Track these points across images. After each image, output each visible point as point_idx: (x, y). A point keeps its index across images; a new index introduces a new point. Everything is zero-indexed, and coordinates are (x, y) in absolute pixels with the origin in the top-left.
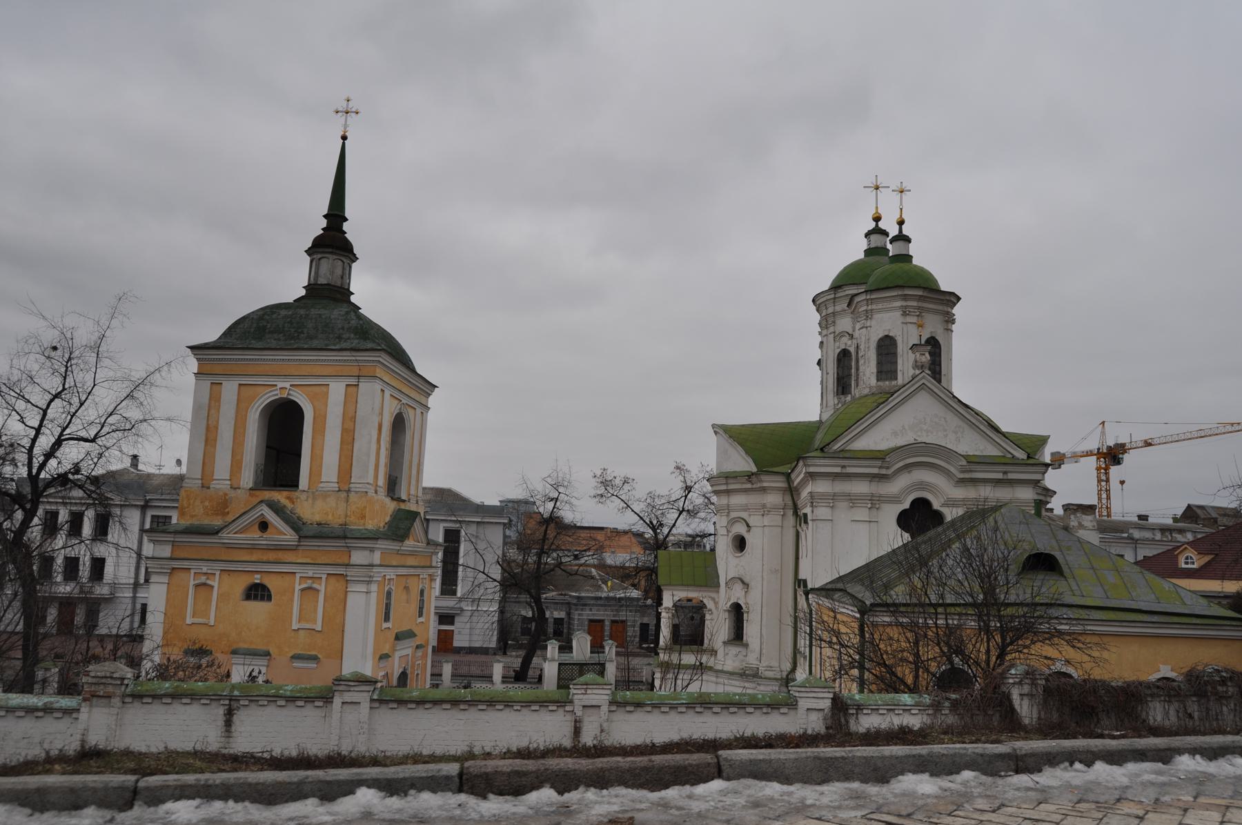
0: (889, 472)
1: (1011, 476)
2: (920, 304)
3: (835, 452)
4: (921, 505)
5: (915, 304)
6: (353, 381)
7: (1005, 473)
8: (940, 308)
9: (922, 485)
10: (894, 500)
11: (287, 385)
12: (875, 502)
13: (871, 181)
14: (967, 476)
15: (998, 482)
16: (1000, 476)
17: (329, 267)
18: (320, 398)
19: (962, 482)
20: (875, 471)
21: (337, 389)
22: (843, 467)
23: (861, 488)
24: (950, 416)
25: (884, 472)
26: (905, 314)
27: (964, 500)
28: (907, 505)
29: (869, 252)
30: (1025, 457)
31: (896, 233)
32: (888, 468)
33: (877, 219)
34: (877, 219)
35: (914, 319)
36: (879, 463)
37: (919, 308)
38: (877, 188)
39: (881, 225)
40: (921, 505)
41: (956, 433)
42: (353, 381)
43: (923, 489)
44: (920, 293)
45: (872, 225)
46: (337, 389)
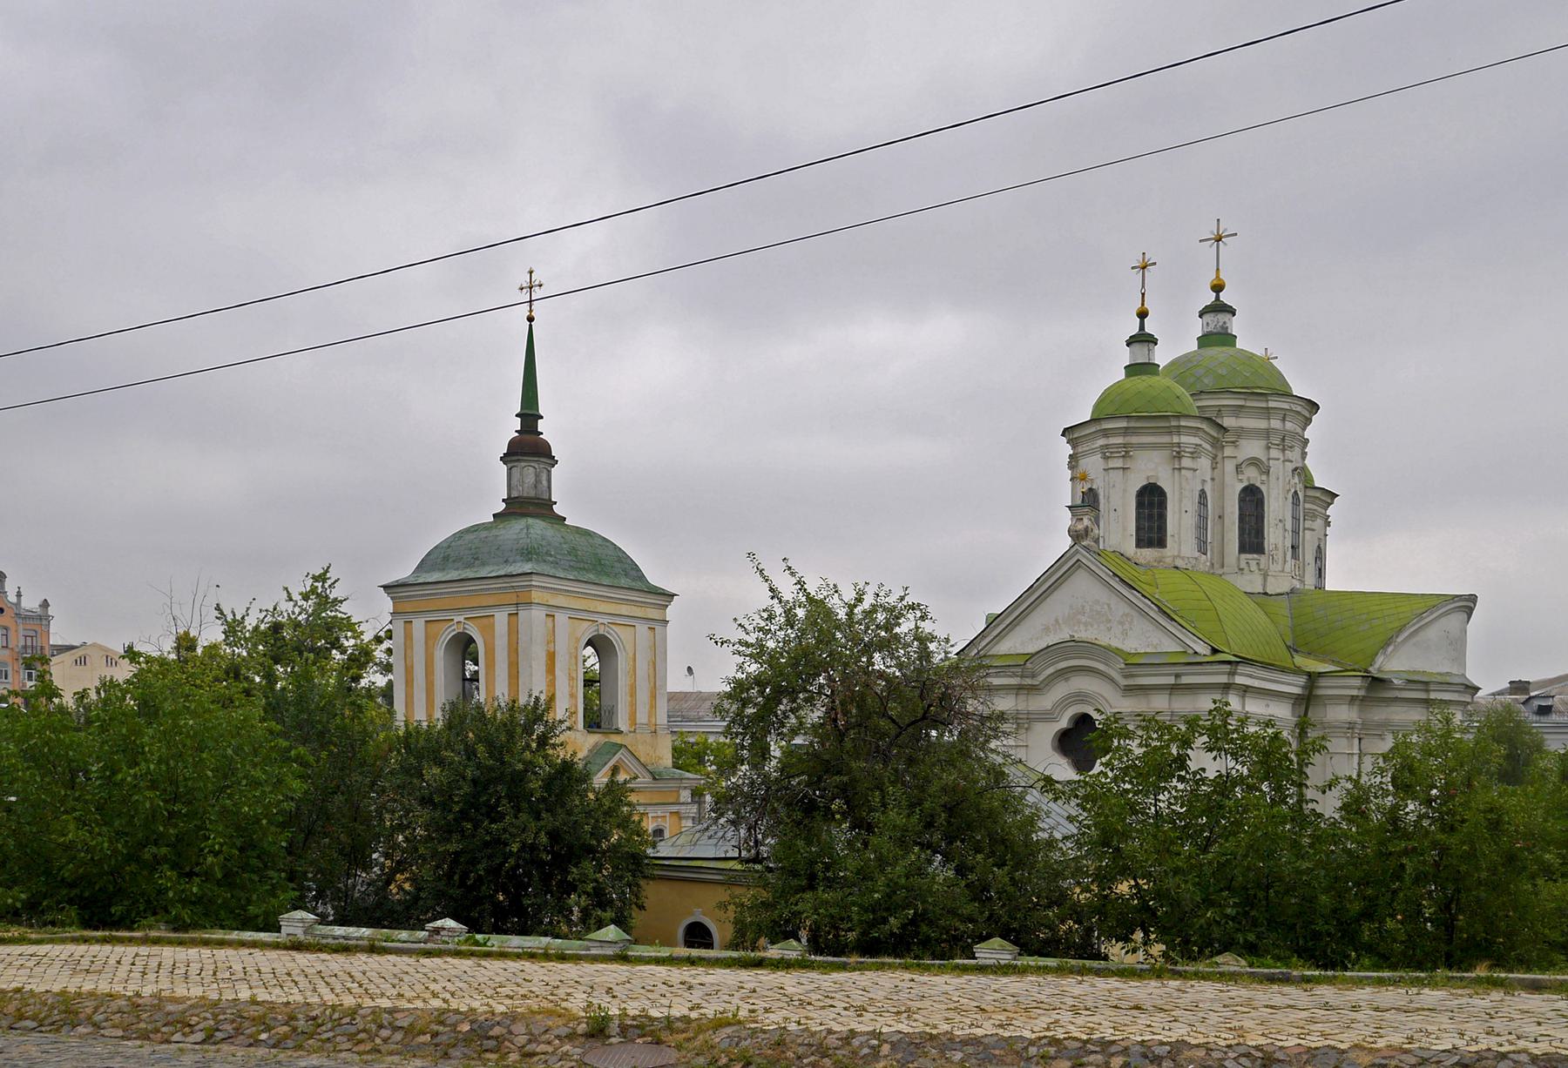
1: (1185, 680)
5: (1119, 440)
6: (513, 610)
7: (1177, 676)
8: (1165, 439)
9: (1080, 697)
10: (1046, 717)
11: (461, 619)
14: (1131, 682)
15: (1174, 689)
16: (1172, 680)
17: (528, 471)
18: (489, 631)
19: (1130, 690)
21: (501, 618)
24: (1114, 601)
25: (1028, 681)
26: (1106, 458)
28: (1064, 723)
29: (1205, 340)
30: (1208, 651)
32: (1033, 676)
35: (1119, 463)
37: (1125, 445)
40: (1083, 721)
41: (1121, 623)
42: (513, 610)
46: (501, 618)
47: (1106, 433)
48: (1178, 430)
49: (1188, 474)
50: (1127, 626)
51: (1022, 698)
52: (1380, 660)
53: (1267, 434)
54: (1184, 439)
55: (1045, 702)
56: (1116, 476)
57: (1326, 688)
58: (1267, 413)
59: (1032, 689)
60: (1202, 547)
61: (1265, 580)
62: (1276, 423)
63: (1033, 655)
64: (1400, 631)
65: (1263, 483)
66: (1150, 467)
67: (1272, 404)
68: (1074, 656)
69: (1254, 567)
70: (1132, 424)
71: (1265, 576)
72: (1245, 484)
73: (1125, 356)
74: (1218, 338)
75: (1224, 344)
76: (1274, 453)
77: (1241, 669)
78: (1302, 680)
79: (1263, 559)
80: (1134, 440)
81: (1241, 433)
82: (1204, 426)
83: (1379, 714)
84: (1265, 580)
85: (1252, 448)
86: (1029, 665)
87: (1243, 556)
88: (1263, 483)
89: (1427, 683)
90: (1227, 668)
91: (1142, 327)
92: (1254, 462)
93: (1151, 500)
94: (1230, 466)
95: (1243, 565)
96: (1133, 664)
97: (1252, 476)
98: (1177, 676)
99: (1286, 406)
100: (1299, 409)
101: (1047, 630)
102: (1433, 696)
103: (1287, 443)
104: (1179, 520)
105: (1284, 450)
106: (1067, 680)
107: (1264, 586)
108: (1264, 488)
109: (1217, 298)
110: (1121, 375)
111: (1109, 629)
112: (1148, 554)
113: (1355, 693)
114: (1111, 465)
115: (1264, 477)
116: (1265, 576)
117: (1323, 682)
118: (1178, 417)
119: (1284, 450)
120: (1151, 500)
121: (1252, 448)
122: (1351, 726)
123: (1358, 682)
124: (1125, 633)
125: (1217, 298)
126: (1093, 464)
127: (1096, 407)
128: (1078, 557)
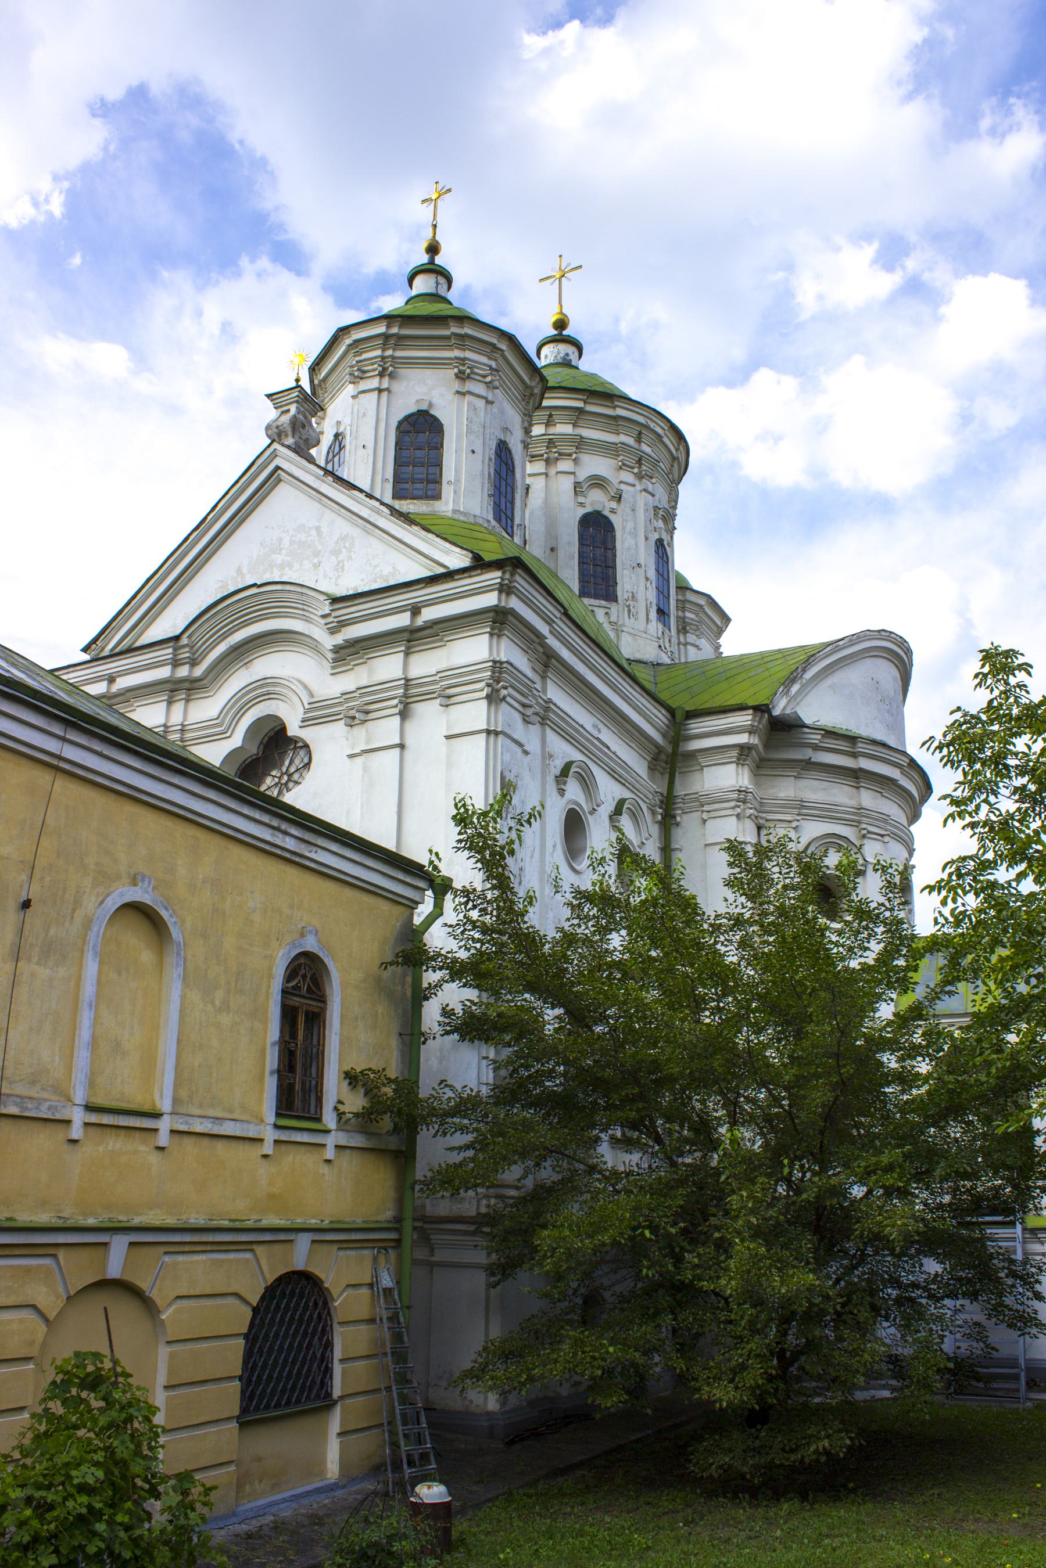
13: (551, 268)
16: (403, 620)
25: (183, 672)
32: (194, 663)
41: (336, 552)
43: (268, 696)
70: (395, 330)
72: (589, 509)
76: (628, 477)
79: (614, 608)
81: (580, 444)
82: (503, 346)
86: (184, 640)
88: (613, 511)
91: (432, 262)
92: (598, 482)
94: (566, 484)
97: (596, 500)
98: (416, 611)
108: (613, 518)
111: (317, 566)
113: (743, 739)
114: (361, 389)
124: (340, 567)
128: (277, 462)
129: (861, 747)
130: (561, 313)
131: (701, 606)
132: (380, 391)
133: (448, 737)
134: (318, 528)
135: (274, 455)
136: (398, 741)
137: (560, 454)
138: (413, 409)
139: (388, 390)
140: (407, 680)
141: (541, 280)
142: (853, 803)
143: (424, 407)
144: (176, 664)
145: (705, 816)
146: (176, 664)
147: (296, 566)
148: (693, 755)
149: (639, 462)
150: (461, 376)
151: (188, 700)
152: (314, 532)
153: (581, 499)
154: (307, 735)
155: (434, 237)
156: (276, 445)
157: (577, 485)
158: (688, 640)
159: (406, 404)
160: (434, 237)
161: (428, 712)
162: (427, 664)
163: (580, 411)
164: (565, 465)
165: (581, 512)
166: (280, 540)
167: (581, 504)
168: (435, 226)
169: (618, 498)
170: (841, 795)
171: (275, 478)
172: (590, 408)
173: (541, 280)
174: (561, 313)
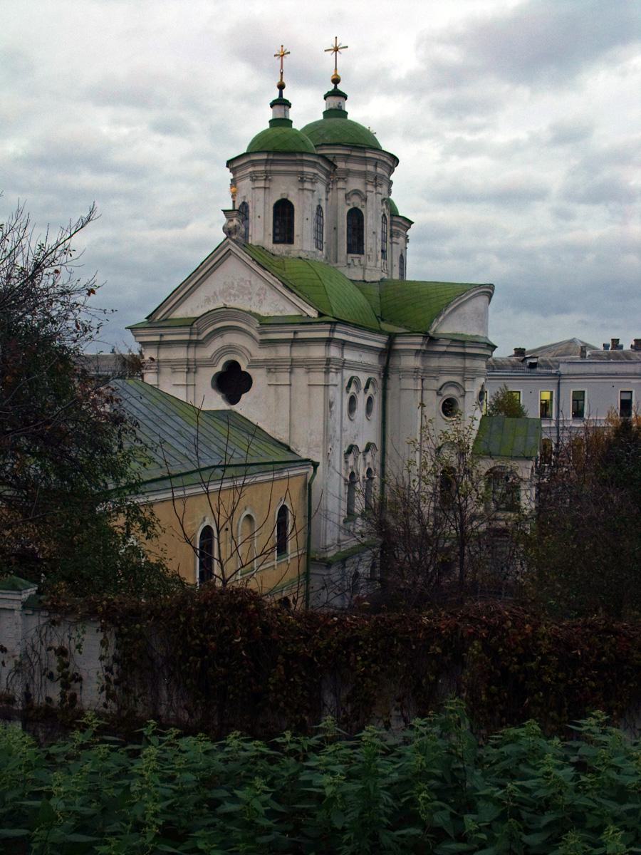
0: (201, 338)
1: (301, 335)
2: (268, 168)
3: (159, 321)
4: (233, 366)
5: (262, 168)
7: (295, 333)
8: (294, 168)
9: (230, 349)
10: (209, 363)
12: (191, 367)
13: (331, 45)
15: (294, 342)
16: (291, 336)
19: (264, 343)
20: (186, 337)
22: (161, 335)
23: (180, 354)
24: (254, 278)
25: (194, 337)
27: (265, 361)
28: (219, 368)
31: (276, 96)
33: (336, 81)
34: (336, 81)
35: (262, 184)
36: (187, 330)
37: (266, 172)
38: (336, 50)
39: (340, 87)
40: (233, 366)
41: (259, 295)
43: (232, 352)
44: (264, 157)
45: (331, 87)
47: (253, 163)
48: (302, 163)
49: (309, 194)
50: (262, 297)
51: (191, 350)
52: (435, 326)
53: (364, 174)
54: (306, 169)
55: (207, 352)
56: (261, 193)
57: (402, 344)
58: (365, 161)
59: (197, 343)
60: (319, 243)
61: (364, 273)
62: (370, 168)
63: (198, 318)
64: (447, 306)
65: (363, 207)
66: (284, 187)
67: (368, 155)
68: (223, 320)
69: (356, 262)
70: (271, 157)
71: (364, 269)
72: (351, 207)
73: (269, 114)
74: (335, 113)
75: (340, 117)
76: (370, 188)
77: (338, 327)
78: (385, 338)
79: (363, 258)
80: (273, 168)
81: (348, 173)
82: (320, 161)
83: (434, 363)
84: (364, 273)
85: (355, 184)
86: (195, 326)
87: (350, 255)
88: (363, 207)
89: (464, 342)
90: (328, 327)
92: (357, 192)
93: (284, 212)
94: (341, 195)
95: (350, 261)
96: (266, 323)
97: (356, 201)
98: (295, 333)
99: (377, 157)
100: (385, 159)
101: (208, 300)
102: (468, 350)
103: (379, 181)
104: (303, 225)
105: (376, 186)
106: (222, 336)
107: (363, 277)
108: (363, 211)
109: (336, 87)
110: (267, 126)
111: (250, 299)
112: (281, 249)
113: (418, 347)
114: (257, 186)
115: (363, 203)
116: (364, 269)
117: (398, 340)
118: (302, 153)
119: (376, 186)
120: (284, 212)
121: (355, 184)
122: (416, 370)
123: (420, 340)
124: (261, 302)
125: (336, 87)
126: (246, 184)
127: (249, 147)
129: (467, 345)
130: (336, 74)
131: (399, 222)
132: (265, 188)
133: (309, 385)
134: (250, 282)
135: (228, 243)
136: (288, 383)
137: (339, 178)
138: (279, 198)
139: (269, 188)
140: (292, 360)
141: (325, 51)
142: (462, 366)
143: (285, 197)
144: (191, 334)
145: (401, 377)
146: (191, 334)
147: (241, 297)
148: (397, 350)
149: (376, 179)
150: (302, 181)
151: (195, 347)
152: (248, 283)
153: (348, 202)
154: (250, 371)
155: (281, 80)
156: (228, 240)
157: (346, 195)
158: (394, 241)
159: (276, 197)
160: (281, 80)
161: (300, 372)
162: (300, 353)
163: (349, 155)
164: (341, 184)
165: (348, 208)
166: (233, 284)
167: (349, 205)
168: (282, 73)
169: (365, 200)
170: (456, 363)
171: (229, 253)
172: (353, 154)
173: (325, 51)
174: (336, 74)
